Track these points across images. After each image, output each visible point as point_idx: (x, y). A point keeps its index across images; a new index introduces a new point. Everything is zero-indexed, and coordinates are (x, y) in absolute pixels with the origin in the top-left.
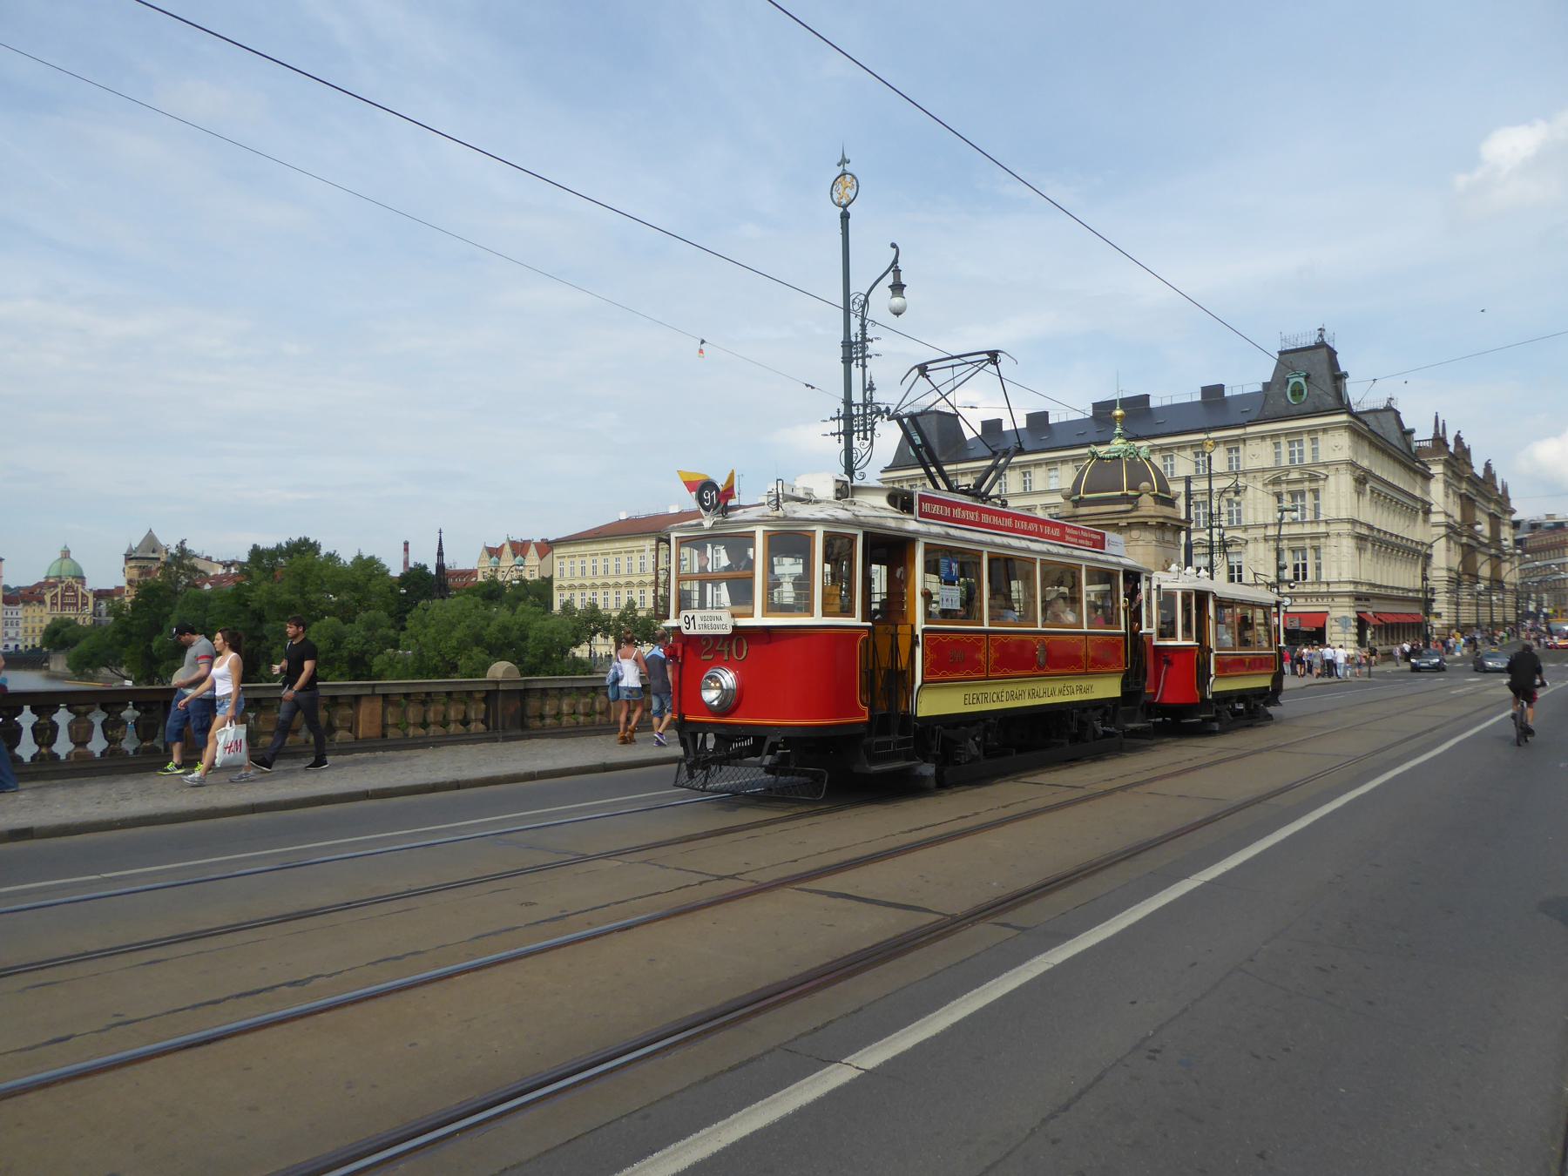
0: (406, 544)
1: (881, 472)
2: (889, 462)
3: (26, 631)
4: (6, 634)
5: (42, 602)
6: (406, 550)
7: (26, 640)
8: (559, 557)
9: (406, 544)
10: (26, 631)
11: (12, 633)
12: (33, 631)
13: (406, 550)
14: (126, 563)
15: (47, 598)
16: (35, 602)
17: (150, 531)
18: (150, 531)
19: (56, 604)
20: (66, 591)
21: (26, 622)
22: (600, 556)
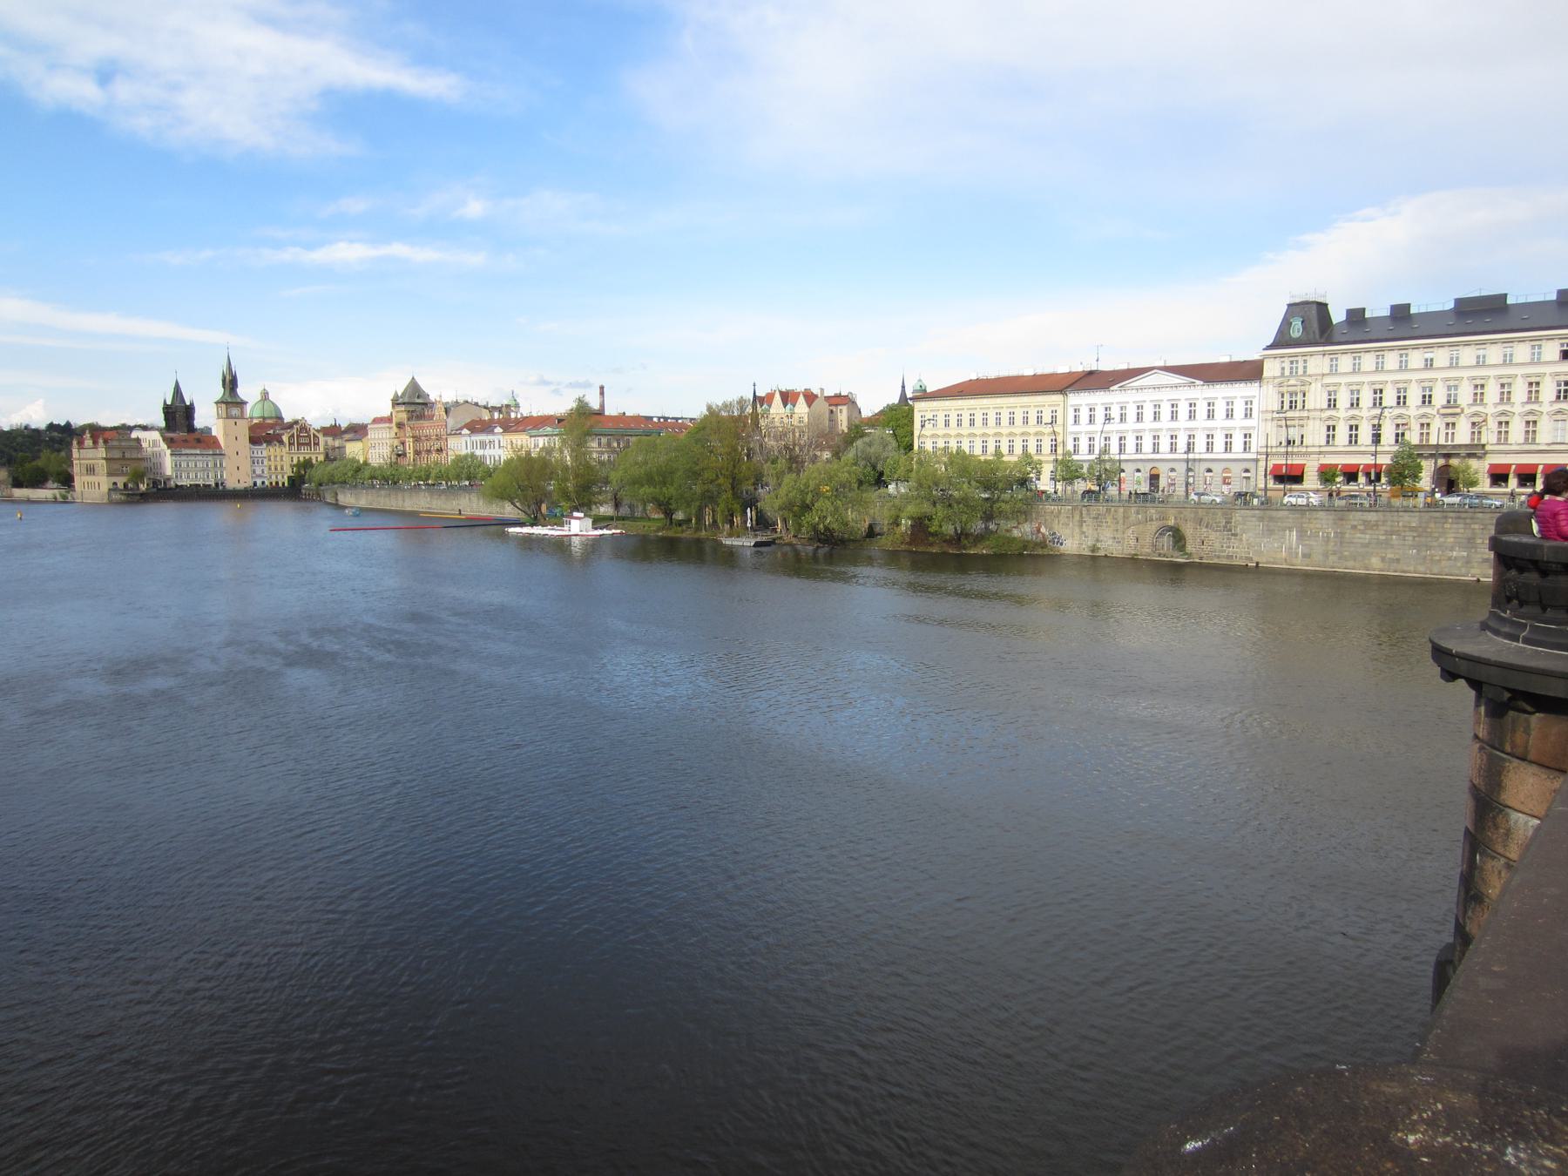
0: (602, 388)
1: (1264, 349)
2: (1270, 341)
3: (270, 469)
4: (254, 472)
5: (281, 442)
6: (602, 393)
7: (271, 477)
8: (920, 411)
9: (602, 388)
10: (270, 469)
11: (258, 472)
12: (276, 469)
13: (602, 393)
14: (393, 407)
15: (285, 438)
16: (275, 442)
17: (413, 378)
18: (413, 378)
19: (293, 444)
20: (301, 432)
21: (270, 460)
22: (965, 410)
